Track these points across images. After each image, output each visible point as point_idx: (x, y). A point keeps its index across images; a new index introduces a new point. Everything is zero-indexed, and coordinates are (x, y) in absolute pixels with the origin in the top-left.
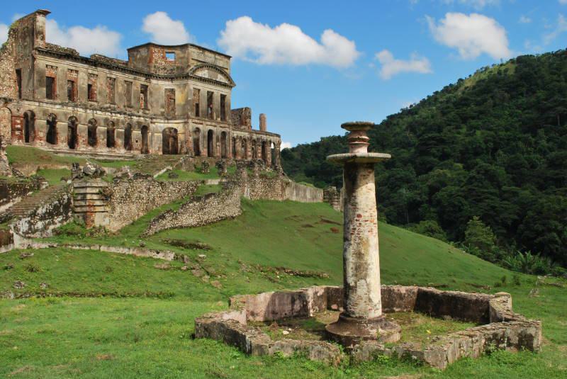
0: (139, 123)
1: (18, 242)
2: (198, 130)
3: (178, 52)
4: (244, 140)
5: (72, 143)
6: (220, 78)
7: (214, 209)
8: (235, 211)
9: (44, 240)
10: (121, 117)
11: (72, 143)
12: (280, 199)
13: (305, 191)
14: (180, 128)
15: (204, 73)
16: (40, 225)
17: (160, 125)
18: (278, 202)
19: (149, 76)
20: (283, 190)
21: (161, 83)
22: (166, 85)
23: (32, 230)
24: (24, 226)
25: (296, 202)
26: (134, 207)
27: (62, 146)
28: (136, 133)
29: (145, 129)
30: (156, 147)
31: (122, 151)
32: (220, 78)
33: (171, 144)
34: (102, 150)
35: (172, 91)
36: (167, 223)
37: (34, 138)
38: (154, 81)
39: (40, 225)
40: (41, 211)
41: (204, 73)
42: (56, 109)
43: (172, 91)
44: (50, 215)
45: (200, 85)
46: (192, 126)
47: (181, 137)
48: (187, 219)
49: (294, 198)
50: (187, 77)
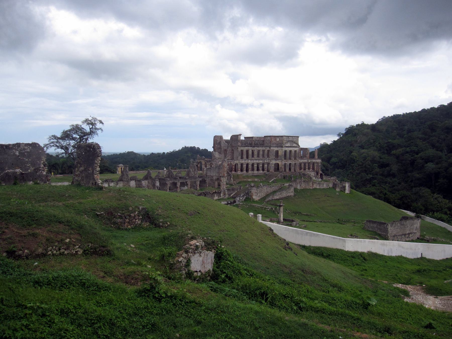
0: (267, 162)
1: (237, 203)
2: (285, 164)
3: (280, 138)
4: (305, 164)
5: (247, 170)
6: (295, 145)
7: (284, 194)
8: (292, 194)
9: (242, 202)
10: (261, 161)
11: (247, 170)
12: (311, 188)
13: (323, 184)
14: (280, 163)
15: (288, 145)
16: (241, 198)
17: (274, 162)
18: (310, 189)
19: (270, 147)
20: (313, 185)
21: (274, 148)
22: (276, 149)
23: (240, 200)
24: (238, 199)
25: (320, 189)
26: (263, 194)
27: (245, 172)
28: (266, 166)
29: (268, 164)
30: (272, 170)
31: (261, 172)
32: (295, 145)
33: (277, 168)
34: (256, 172)
35: (278, 151)
36: (270, 198)
37: (238, 170)
38: (272, 148)
39: (241, 198)
40: (242, 195)
41: (288, 145)
42: (243, 162)
43: (278, 151)
44: (243, 196)
45: (287, 149)
46: (283, 163)
47: (280, 166)
48: (276, 197)
49: (318, 187)
50: (282, 147)
